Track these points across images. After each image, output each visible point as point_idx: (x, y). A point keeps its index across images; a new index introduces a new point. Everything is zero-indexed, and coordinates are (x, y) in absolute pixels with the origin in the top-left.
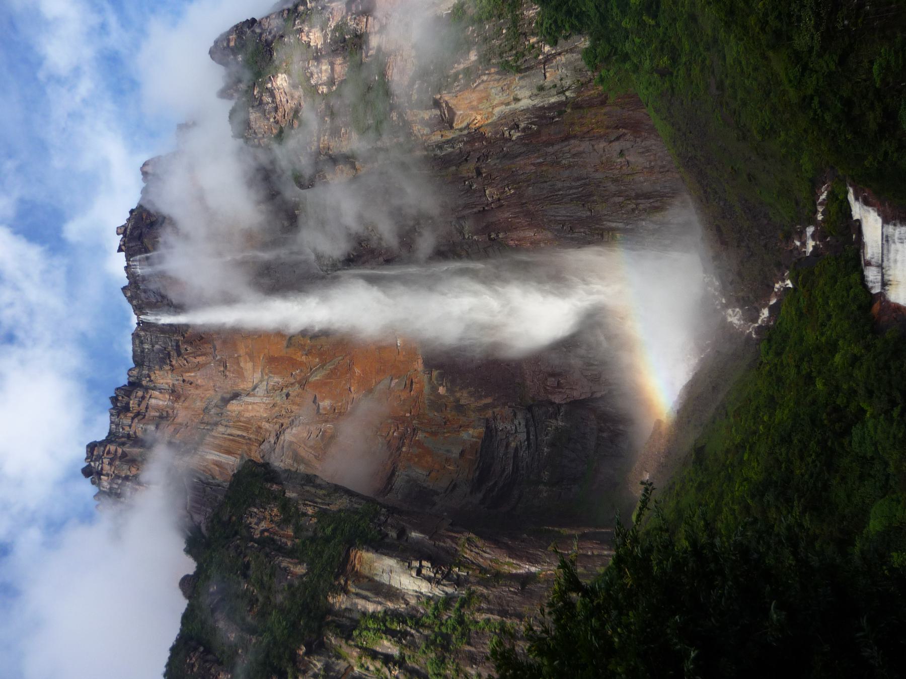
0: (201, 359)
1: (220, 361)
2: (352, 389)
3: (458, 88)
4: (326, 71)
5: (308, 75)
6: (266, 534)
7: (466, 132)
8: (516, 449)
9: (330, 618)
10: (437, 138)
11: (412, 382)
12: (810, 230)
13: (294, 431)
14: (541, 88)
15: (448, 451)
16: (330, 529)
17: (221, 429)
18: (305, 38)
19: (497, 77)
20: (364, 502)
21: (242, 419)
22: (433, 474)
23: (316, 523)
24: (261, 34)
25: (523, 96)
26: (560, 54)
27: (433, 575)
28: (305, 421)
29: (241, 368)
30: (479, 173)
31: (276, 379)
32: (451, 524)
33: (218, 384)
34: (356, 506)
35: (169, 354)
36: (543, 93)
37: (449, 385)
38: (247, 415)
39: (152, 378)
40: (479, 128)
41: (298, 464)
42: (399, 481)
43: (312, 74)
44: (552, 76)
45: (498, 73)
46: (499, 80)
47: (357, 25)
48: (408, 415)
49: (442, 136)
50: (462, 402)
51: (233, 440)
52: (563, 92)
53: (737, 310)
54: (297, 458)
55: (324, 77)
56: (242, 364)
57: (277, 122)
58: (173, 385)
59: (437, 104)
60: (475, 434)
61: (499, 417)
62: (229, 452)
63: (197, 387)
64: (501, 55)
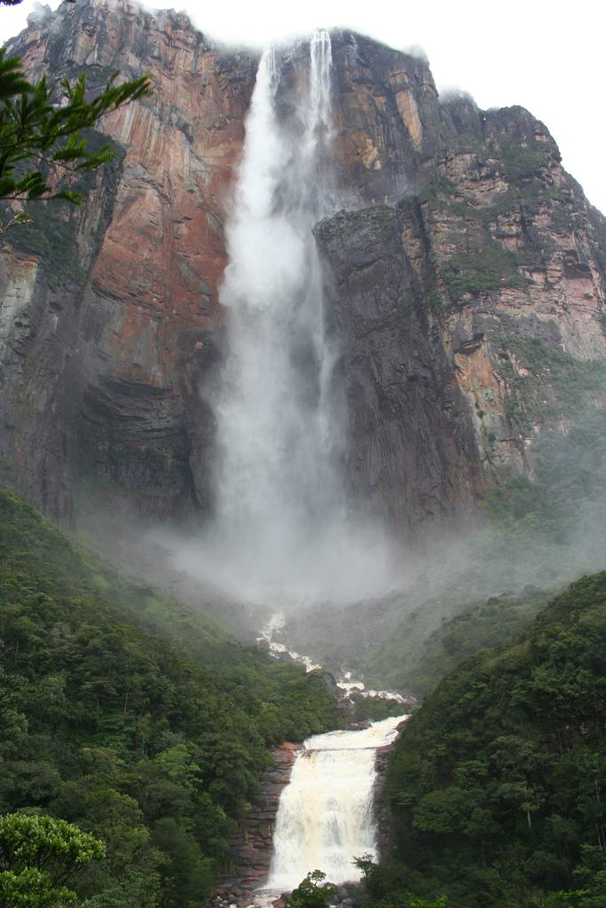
0: (226, 103)
1: (226, 124)
2: (199, 256)
3: (493, 358)
4: (511, 230)
5: (507, 213)
6: (51, 170)
7: (451, 365)
8: (142, 419)
10: (445, 337)
11: (206, 315)
12: (361, 686)
13: (156, 199)
14: (492, 439)
15: (139, 351)
16: (59, 235)
17: (157, 124)
18: (542, 210)
19: (503, 395)
20: (86, 269)
21: (167, 146)
22: (116, 337)
23: (64, 221)
24: (546, 167)
25: (485, 421)
26: (523, 454)
27: (17, 338)
28: (166, 210)
29: (218, 144)
30: (412, 379)
31: (208, 180)
32: (67, 356)
33: (201, 121)
34: (83, 261)
35: (231, 71)
36: (487, 439)
37: (205, 352)
38: (171, 150)
39: (207, 54)
40: (455, 377)
41: (123, 203)
42: (108, 304)
43: (508, 216)
44: (502, 447)
45: (506, 397)
46: (500, 397)
47: (554, 261)
48: (174, 312)
49: (447, 342)
50: (188, 365)
51: (146, 133)
52: (487, 458)
53: (284, 623)
54: (130, 201)
55: (505, 229)
56: (222, 146)
57: (461, 181)
58: (200, 75)
59: (478, 337)
60: (156, 378)
61: (175, 401)
62: (133, 132)
63: (199, 100)
64: (521, 399)
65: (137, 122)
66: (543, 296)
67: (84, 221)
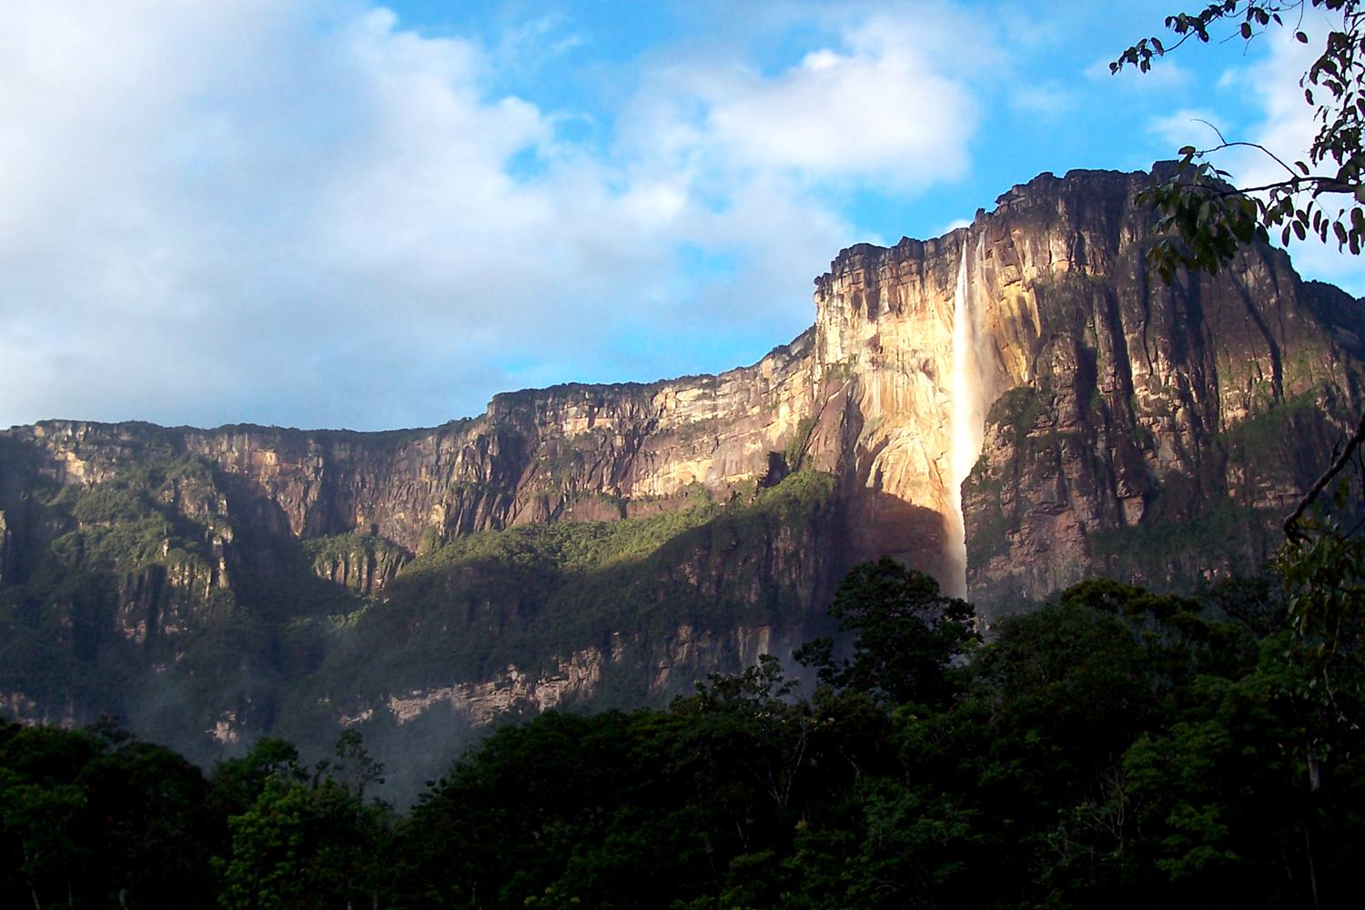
9: (732, 632)
13: (918, 447)
17: (900, 380)
39: (930, 272)
51: (893, 398)
65: (884, 390)
66: (1019, 552)
67: (800, 575)
